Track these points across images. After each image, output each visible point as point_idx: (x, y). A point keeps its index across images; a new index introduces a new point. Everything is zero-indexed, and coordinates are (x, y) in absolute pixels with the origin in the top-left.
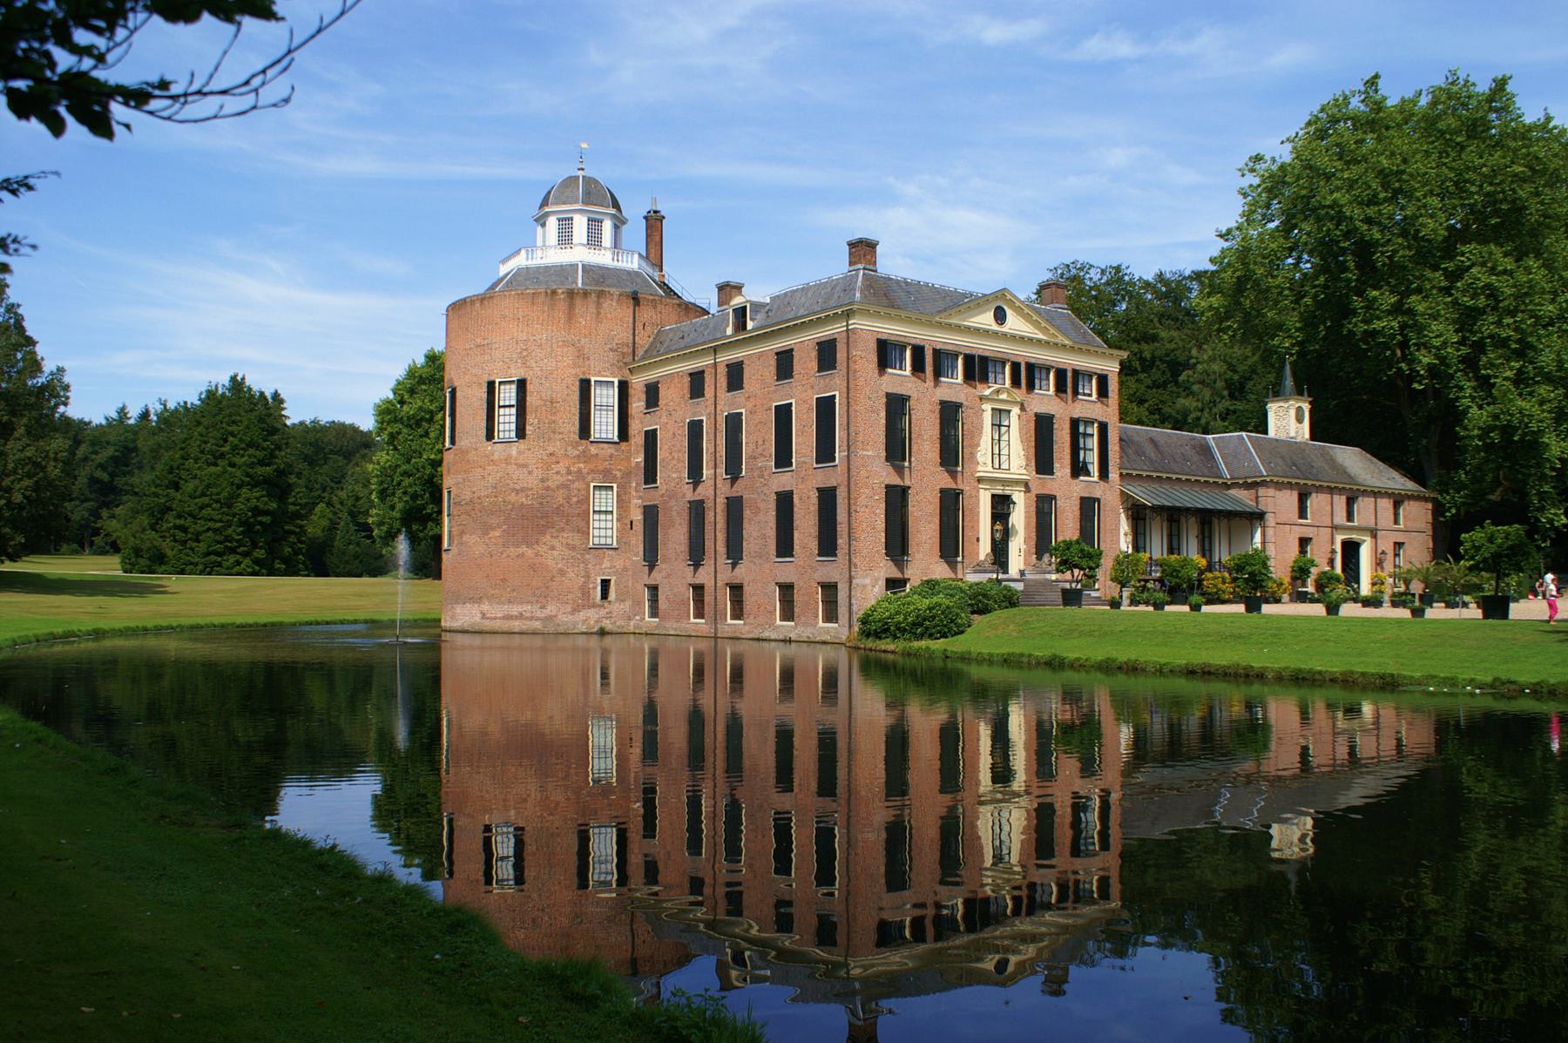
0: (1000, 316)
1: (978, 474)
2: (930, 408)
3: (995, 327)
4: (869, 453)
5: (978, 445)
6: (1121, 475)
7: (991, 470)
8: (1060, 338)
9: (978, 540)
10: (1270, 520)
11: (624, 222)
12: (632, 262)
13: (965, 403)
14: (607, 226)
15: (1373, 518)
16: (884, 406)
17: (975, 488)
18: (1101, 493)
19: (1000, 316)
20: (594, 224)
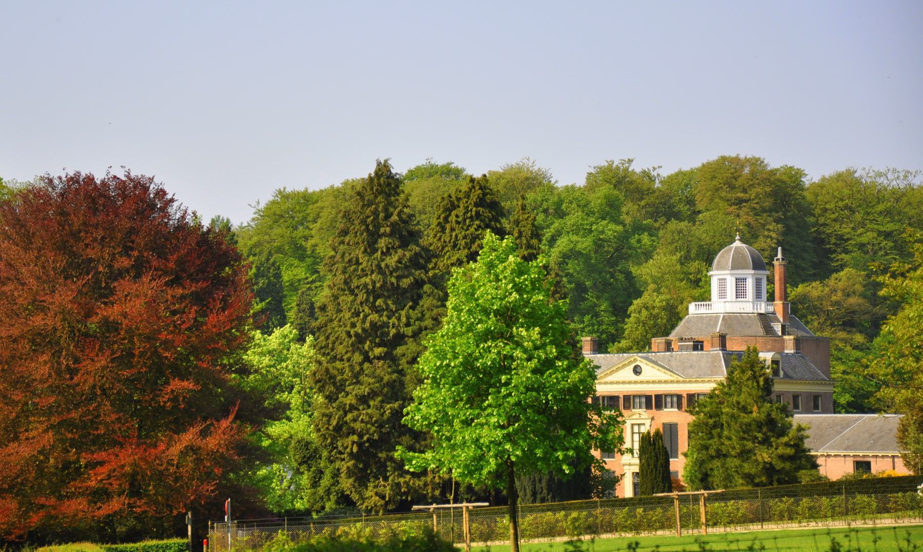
0: (637, 371)
19: (637, 371)
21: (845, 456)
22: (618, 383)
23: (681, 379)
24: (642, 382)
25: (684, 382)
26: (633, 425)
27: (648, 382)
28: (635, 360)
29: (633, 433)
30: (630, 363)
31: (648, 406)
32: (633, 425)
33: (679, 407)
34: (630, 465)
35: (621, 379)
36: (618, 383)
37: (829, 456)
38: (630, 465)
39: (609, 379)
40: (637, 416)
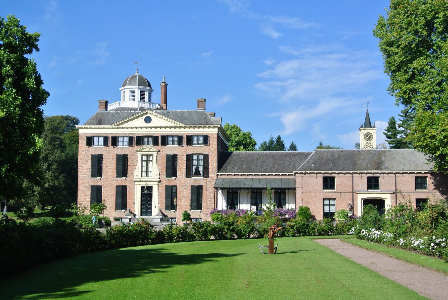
0: (148, 120)
1: (134, 179)
2: (112, 157)
3: (146, 125)
4: (84, 175)
5: (135, 169)
6: (218, 175)
7: (140, 177)
8: (179, 123)
9: (134, 203)
10: (298, 191)
11: (152, 91)
12: (151, 107)
13: (129, 154)
14: (146, 94)
15: (395, 186)
16: (91, 159)
17: (133, 184)
18: (204, 183)
19: (148, 120)
20: (142, 92)
21: (317, 173)
22: (132, 128)
23: (183, 125)
24: (152, 128)
25: (185, 128)
26: (142, 155)
27: (156, 127)
28: (147, 113)
29: (142, 161)
30: (144, 114)
31: (156, 143)
32: (142, 155)
33: (180, 143)
34: (140, 181)
35: (136, 125)
36: (132, 128)
37: (305, 174)
38: (140, 181)
39: (126, 125)
40: (147, 150)
